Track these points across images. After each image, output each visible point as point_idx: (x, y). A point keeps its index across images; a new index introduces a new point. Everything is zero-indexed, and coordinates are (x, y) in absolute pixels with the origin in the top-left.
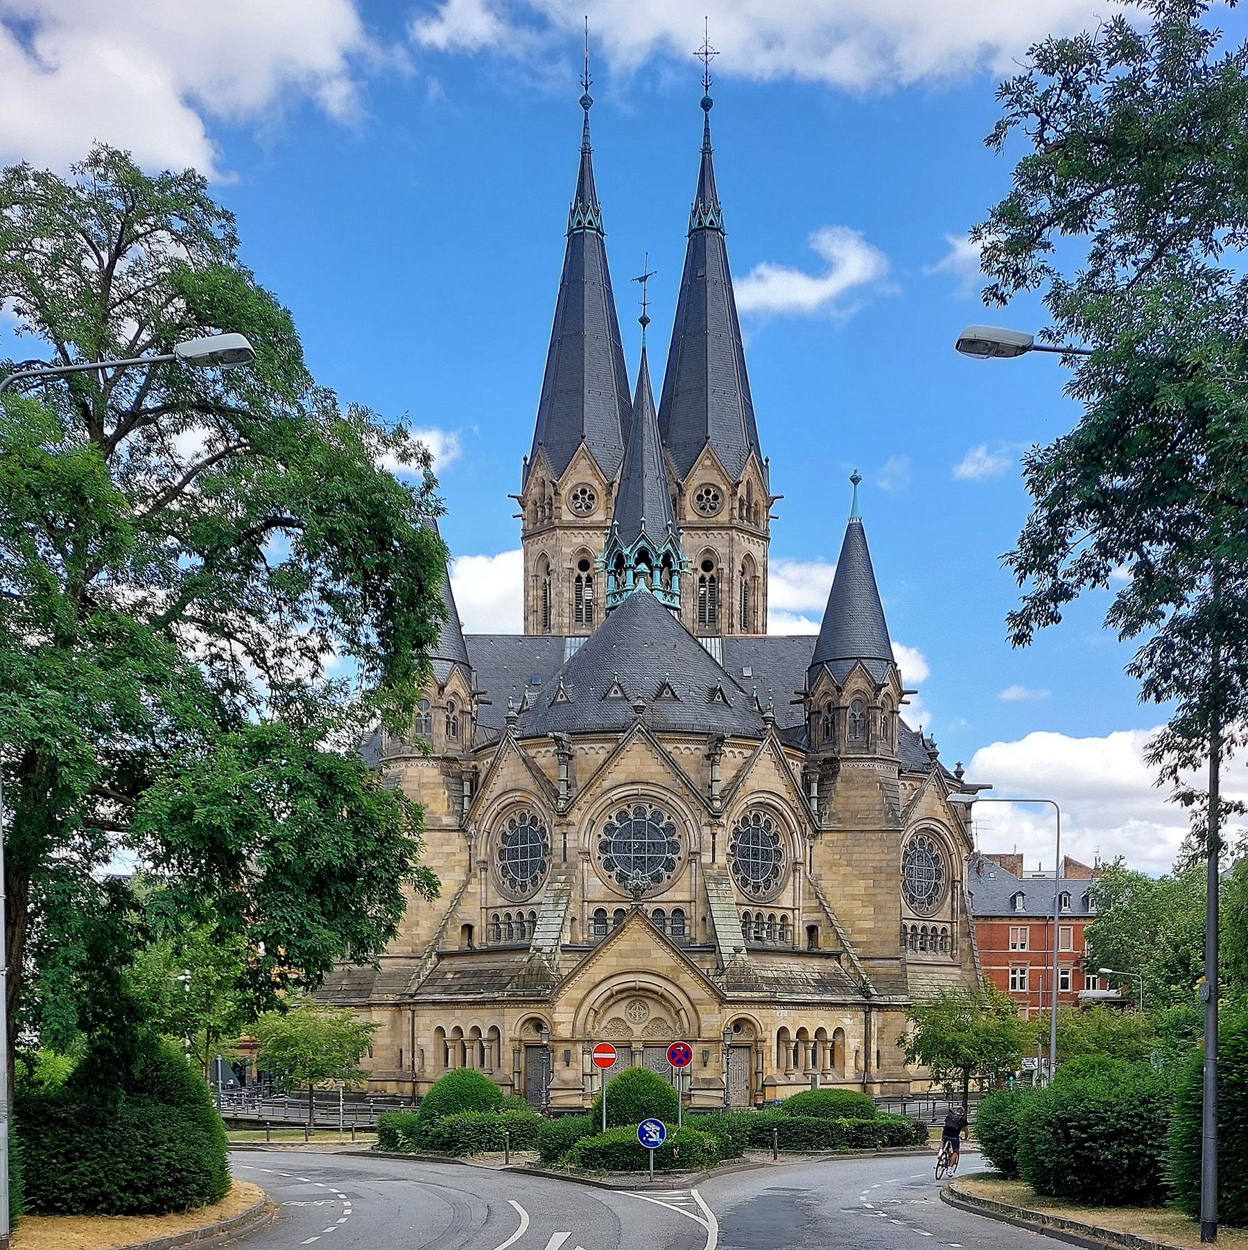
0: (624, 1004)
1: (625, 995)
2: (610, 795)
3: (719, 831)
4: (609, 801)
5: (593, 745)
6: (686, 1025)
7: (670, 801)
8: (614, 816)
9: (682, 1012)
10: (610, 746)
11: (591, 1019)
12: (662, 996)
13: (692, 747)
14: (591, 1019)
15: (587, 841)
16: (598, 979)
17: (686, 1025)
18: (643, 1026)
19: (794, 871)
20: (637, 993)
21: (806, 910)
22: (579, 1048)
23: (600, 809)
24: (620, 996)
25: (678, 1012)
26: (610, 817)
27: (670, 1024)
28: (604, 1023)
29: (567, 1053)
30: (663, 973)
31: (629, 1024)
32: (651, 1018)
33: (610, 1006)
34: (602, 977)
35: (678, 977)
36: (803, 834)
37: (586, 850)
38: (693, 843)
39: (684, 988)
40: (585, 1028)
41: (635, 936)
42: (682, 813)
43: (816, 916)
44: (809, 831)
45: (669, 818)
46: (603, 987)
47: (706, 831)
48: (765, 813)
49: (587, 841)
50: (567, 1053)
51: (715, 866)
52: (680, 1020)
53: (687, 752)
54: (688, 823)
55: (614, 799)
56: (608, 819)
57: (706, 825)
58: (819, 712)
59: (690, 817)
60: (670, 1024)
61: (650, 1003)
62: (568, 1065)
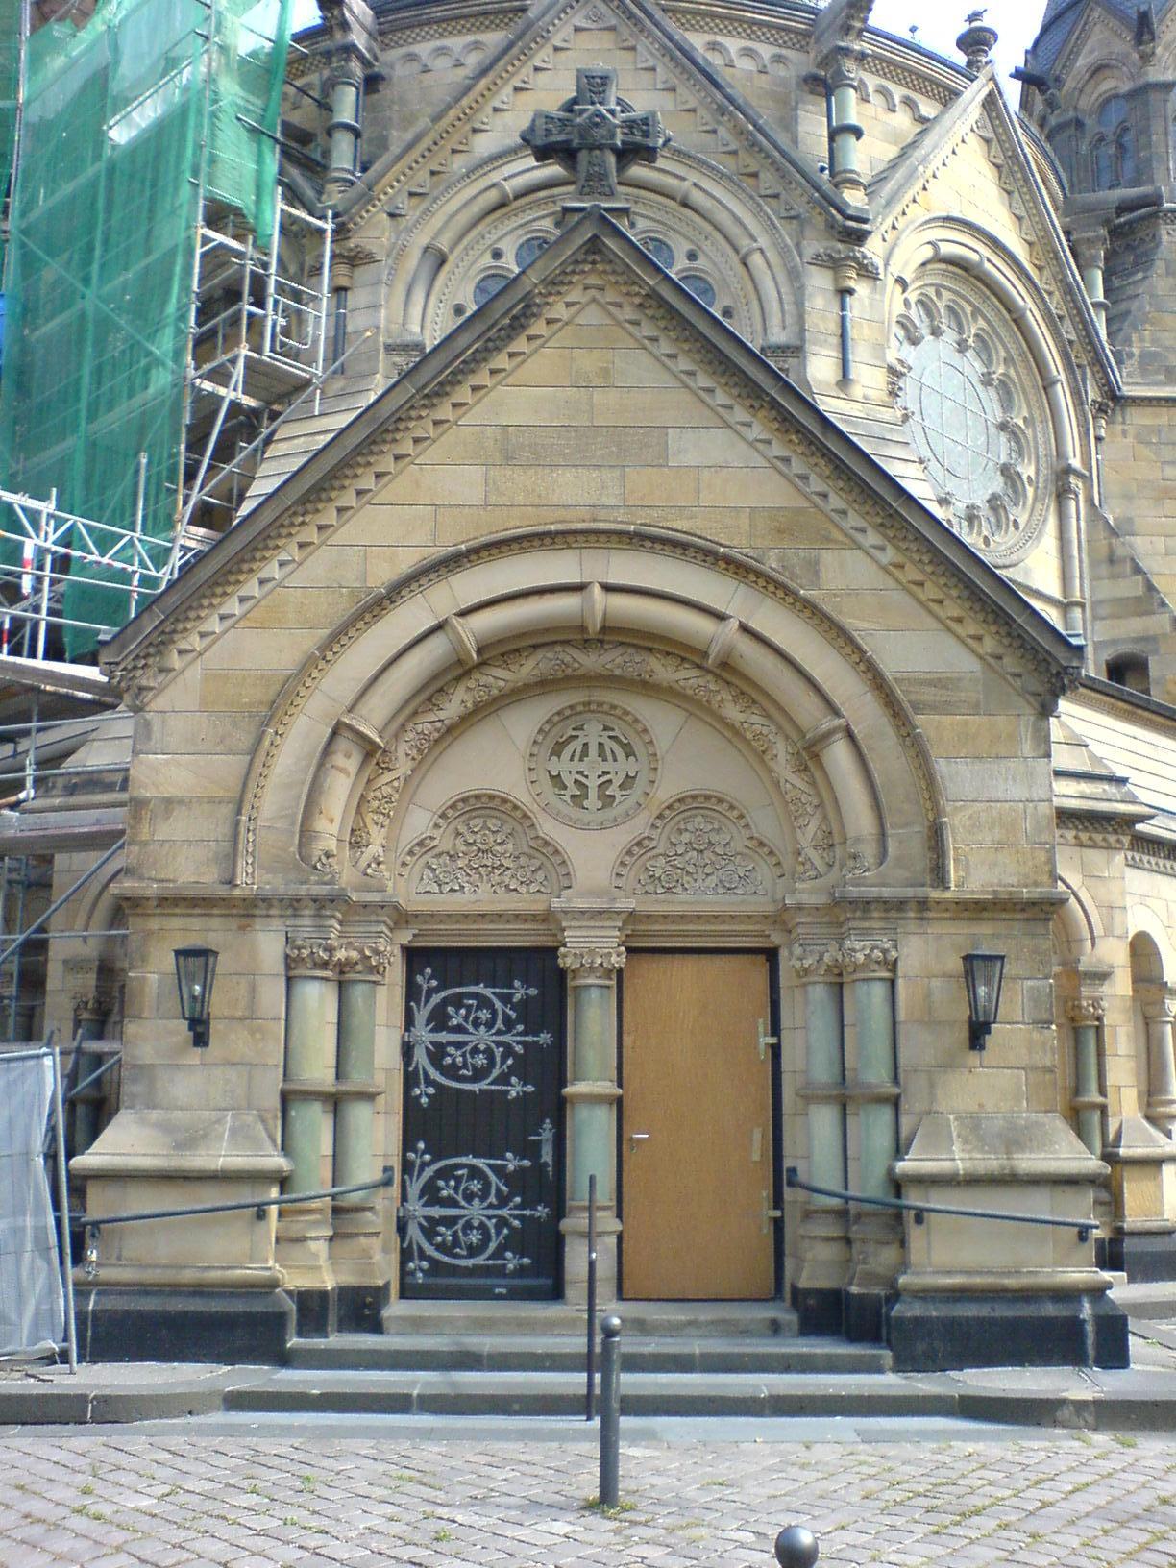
0: (524, 723)
1: (528, 669)
2: (496, 177)
3: (862, 289)
4: (493, 196)
5: (448, 42)
6: (860, 818)
7: (697, 197)
8: (509, 247)
9: (839, 754)
10: (494, 38)
11: (340, 790)
12: (727, 669)
13: (766, 51)
14: (340, 790)
15: (416, 311)
16: (383, 574)
17: (860, 818)
18: (623, 836)
19: (1062, 494)
20: (590, 661)
21: (1103, 611)
22: (269, 944)
23: (463, 219)
24: (499, 678)
25: (810, 754)
26: (497, 255)
27: (766, 824)
28: (419, 822)
29: (197, 959)
30: (738, 542)
31: (548, 828)
32: (667, 791)
33: (453, 731)
34: (407, 561)
35: (813, 567)
36: (1078, 395)
37: (408, 339)
38: (775, 319)
39: (849, 622)
40: (307, 834)
41: (588, 362)
42: (734, 230)
43: (1135, 626)
44: (1092, 394)
45: (692, 256)
46: (411, 617)
47: (819, 282)
48: (976, 312)
49: (416, 311)
50: (197, 959)
51: (857, 391)
52: (828, 803)
53: (745, 64)
54: (756, 260)
55: (510, 187)
56: (487, 260)
57: (818, 261)
58: (1079, 124)
59: (763, 241)
60: (766, 824)
61: (661, 721)
62: (200, 1039)
